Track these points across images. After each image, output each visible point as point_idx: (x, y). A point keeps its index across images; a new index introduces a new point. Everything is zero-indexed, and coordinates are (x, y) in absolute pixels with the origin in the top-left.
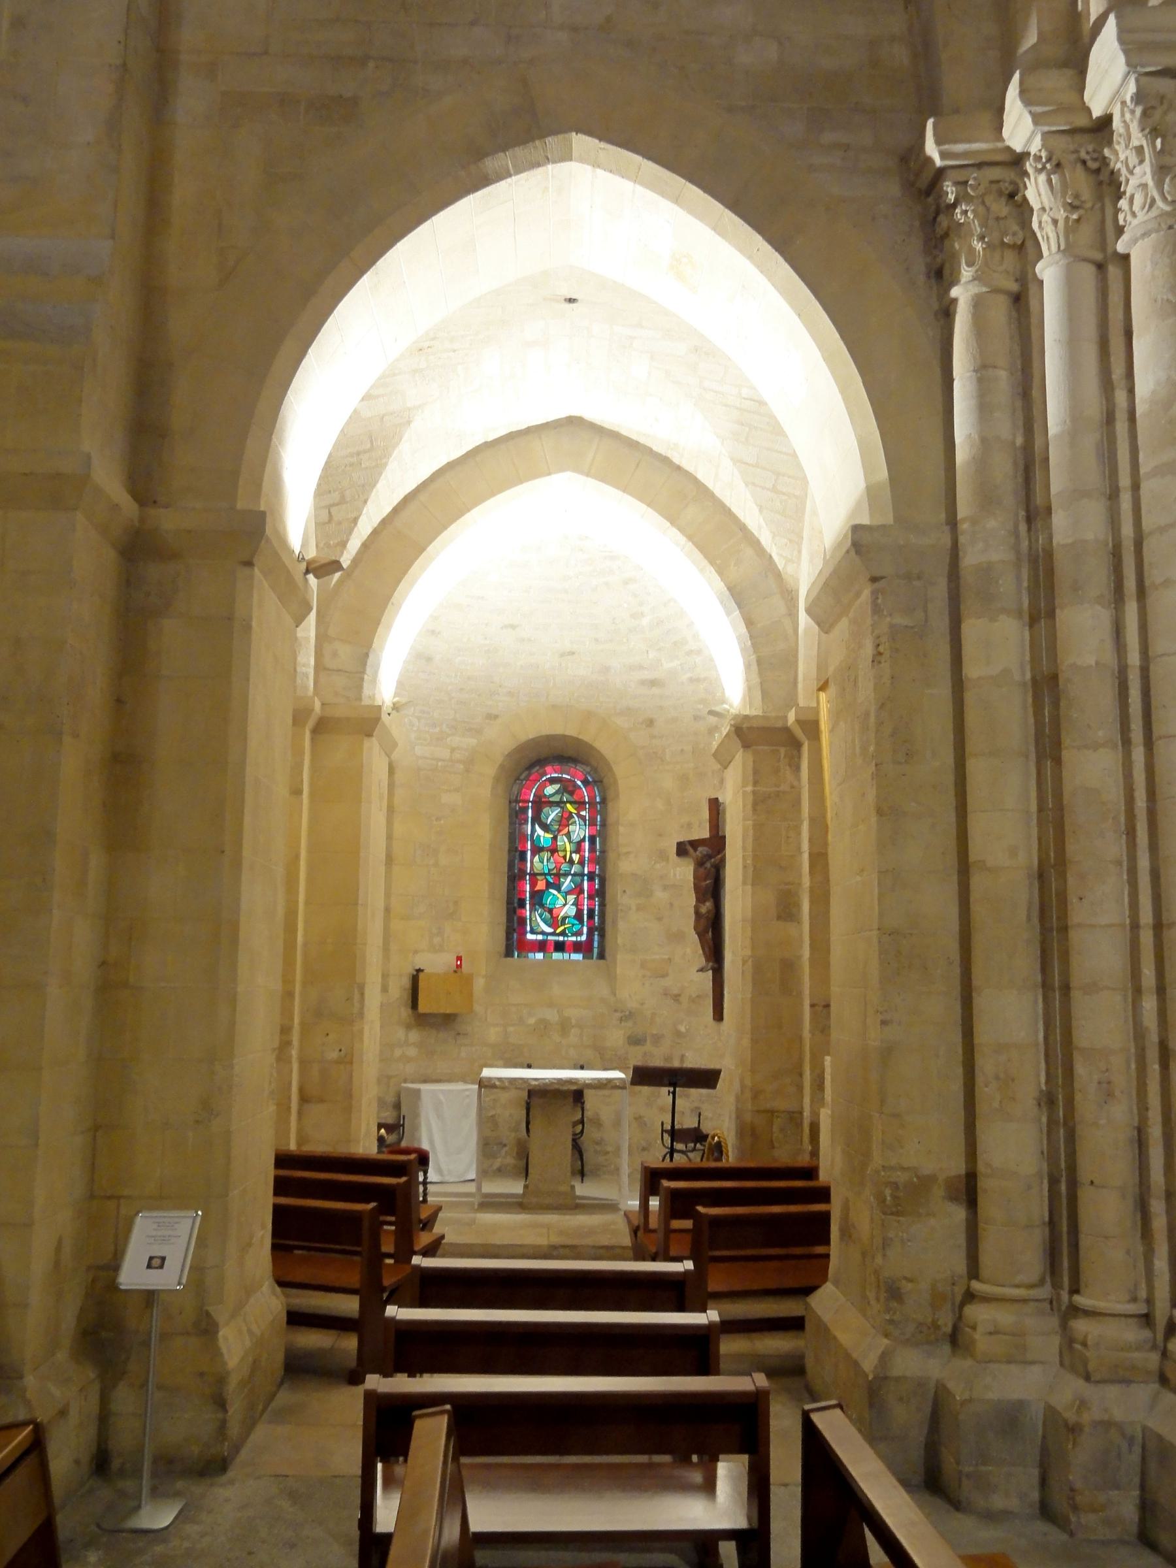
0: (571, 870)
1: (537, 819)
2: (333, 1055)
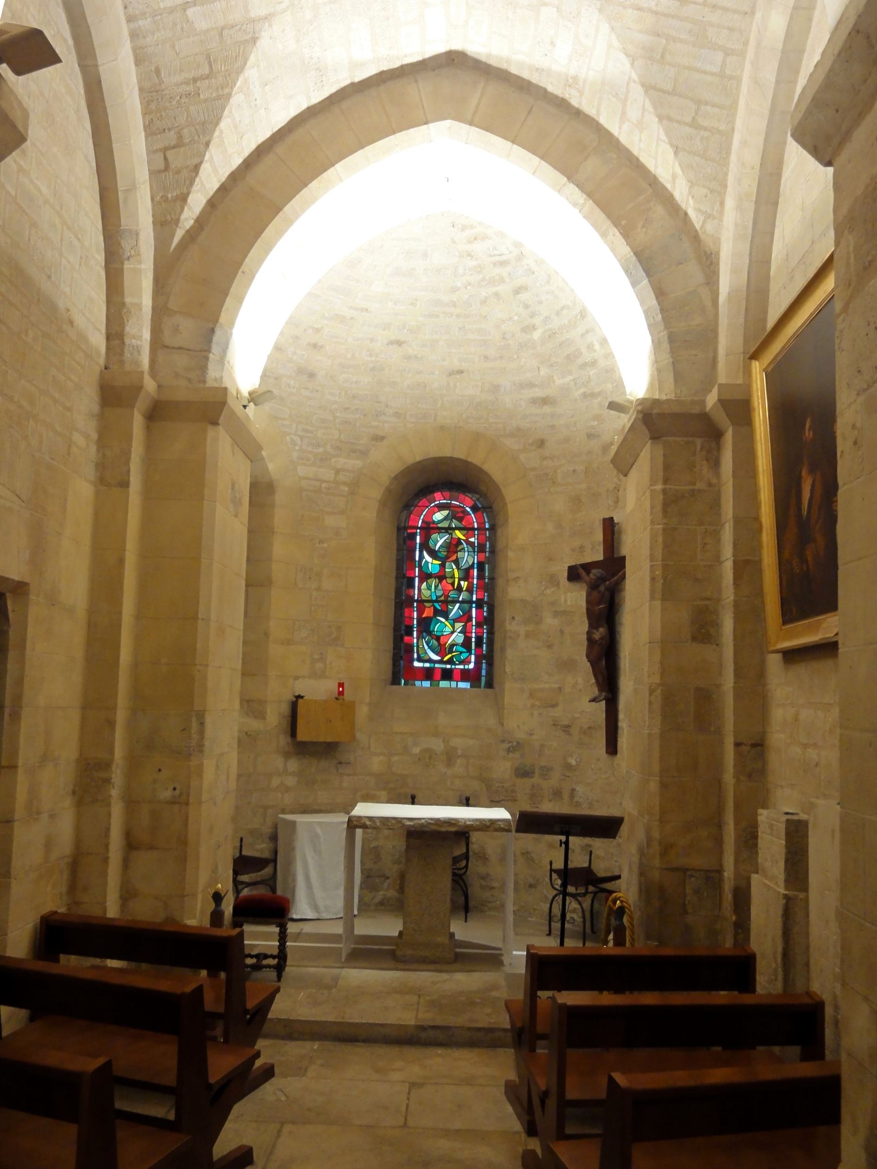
0: (459, 598)
1: (425, 546)
2: (167, 794)
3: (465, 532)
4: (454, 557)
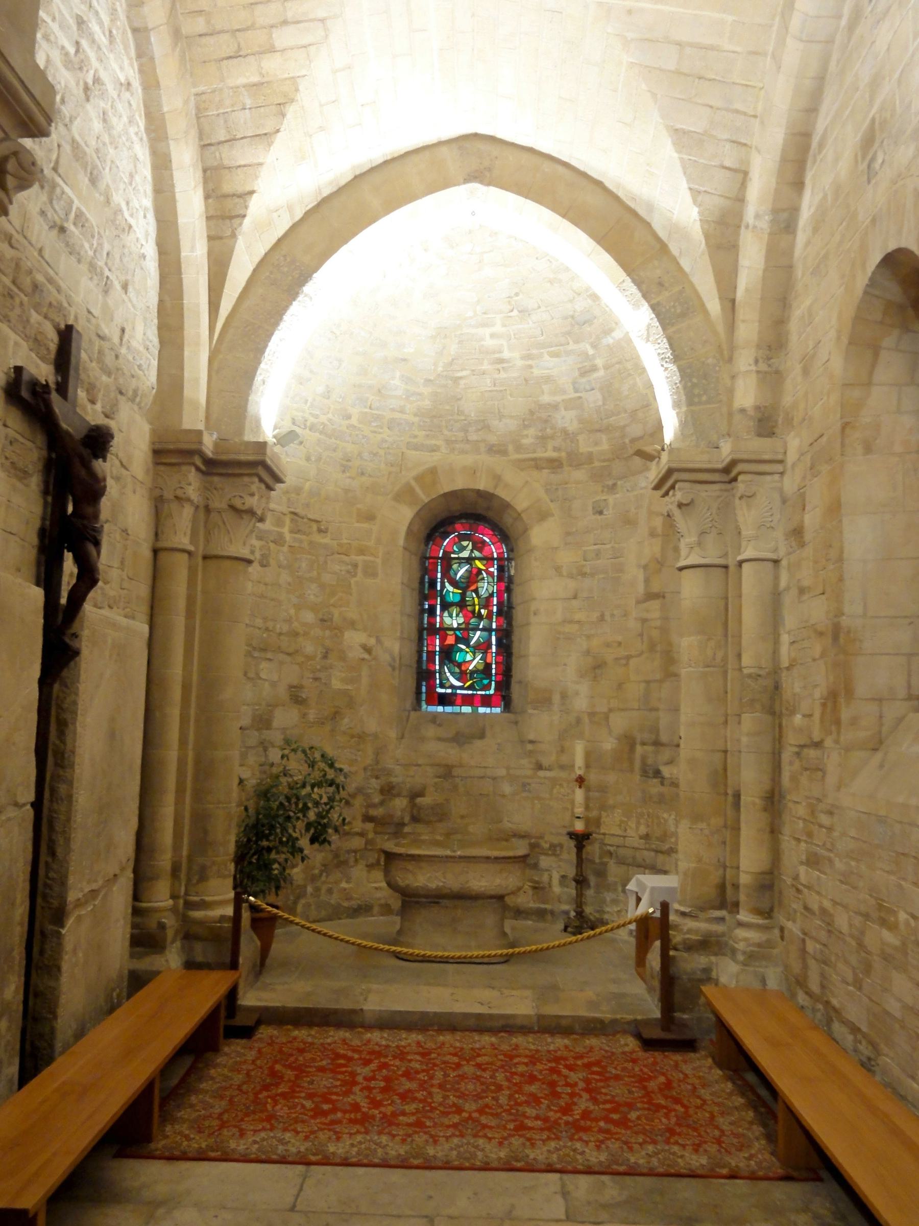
3: (485, 562)
4: (473, 588)
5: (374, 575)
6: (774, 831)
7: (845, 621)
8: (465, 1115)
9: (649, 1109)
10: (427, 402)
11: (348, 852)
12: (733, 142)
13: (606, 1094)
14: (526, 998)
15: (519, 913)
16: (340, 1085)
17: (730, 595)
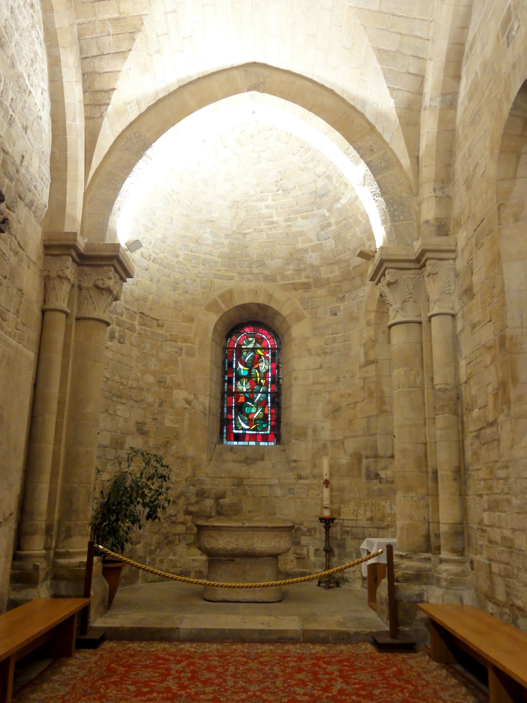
3: (263, 351)
4: (256, 366)
5: (193, 355)
6: (462, 494)
7: (509, 332)
8: (251, 693)
9: (387, 688)
10: (227, 249)
11: (174, 535)
12: (415, 56)
13: (355, 679)
14: (294, 620)
15: (288, 575)
16: (158, 676)
17: (423, 340)
